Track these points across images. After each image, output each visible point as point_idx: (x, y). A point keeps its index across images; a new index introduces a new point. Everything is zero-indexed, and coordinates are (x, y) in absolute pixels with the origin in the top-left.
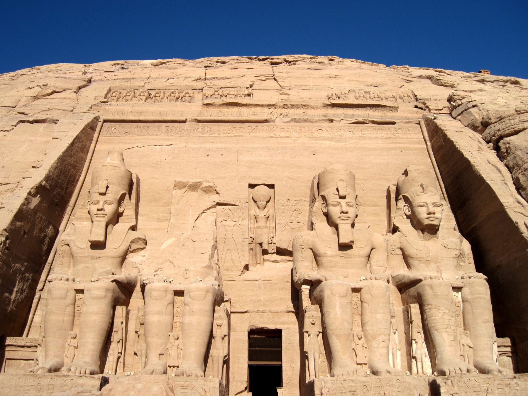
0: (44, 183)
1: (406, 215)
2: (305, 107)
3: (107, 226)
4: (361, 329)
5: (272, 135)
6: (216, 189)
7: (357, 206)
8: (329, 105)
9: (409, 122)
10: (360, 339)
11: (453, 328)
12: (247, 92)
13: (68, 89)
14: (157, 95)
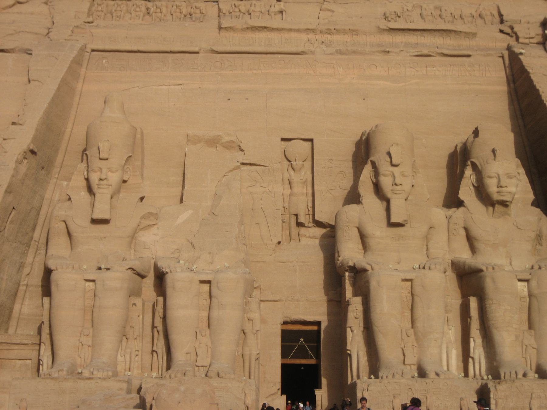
0: (31, 148)
1: (474, 186)
2: (355, 33)
3: (111, 198)
4: (410, 326)
6: (241, 144)
8: (384, 30)
9: (488, 55)
11: (514, 326)
14: (158, 10)
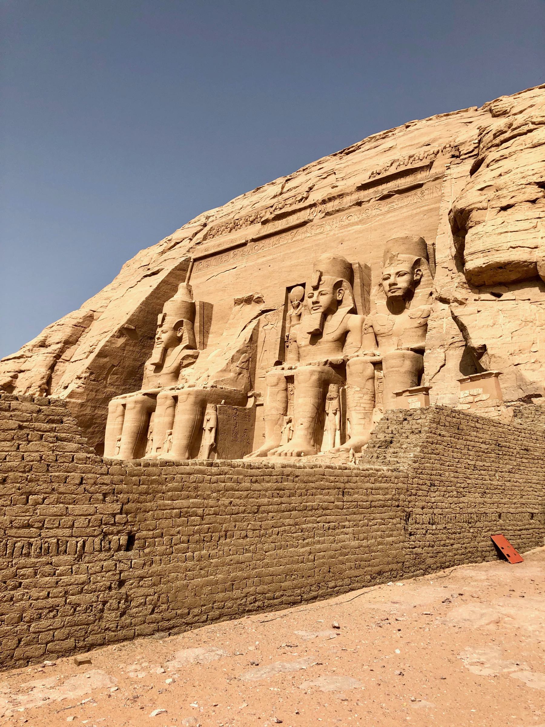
5: (309, 235)
7: (341, 291)
10: (287, 423)
11: (362, 405)
12: (300, 198)
13: (186, 238)
